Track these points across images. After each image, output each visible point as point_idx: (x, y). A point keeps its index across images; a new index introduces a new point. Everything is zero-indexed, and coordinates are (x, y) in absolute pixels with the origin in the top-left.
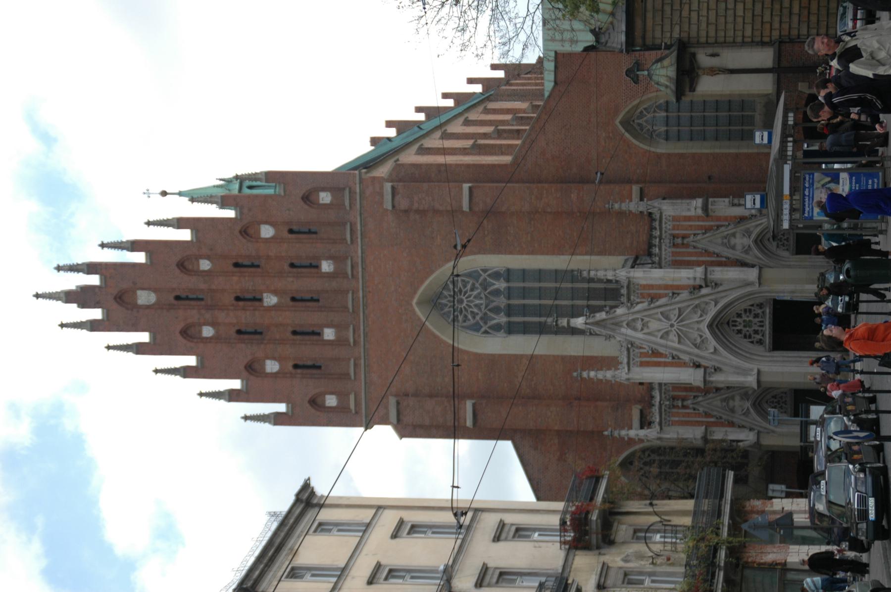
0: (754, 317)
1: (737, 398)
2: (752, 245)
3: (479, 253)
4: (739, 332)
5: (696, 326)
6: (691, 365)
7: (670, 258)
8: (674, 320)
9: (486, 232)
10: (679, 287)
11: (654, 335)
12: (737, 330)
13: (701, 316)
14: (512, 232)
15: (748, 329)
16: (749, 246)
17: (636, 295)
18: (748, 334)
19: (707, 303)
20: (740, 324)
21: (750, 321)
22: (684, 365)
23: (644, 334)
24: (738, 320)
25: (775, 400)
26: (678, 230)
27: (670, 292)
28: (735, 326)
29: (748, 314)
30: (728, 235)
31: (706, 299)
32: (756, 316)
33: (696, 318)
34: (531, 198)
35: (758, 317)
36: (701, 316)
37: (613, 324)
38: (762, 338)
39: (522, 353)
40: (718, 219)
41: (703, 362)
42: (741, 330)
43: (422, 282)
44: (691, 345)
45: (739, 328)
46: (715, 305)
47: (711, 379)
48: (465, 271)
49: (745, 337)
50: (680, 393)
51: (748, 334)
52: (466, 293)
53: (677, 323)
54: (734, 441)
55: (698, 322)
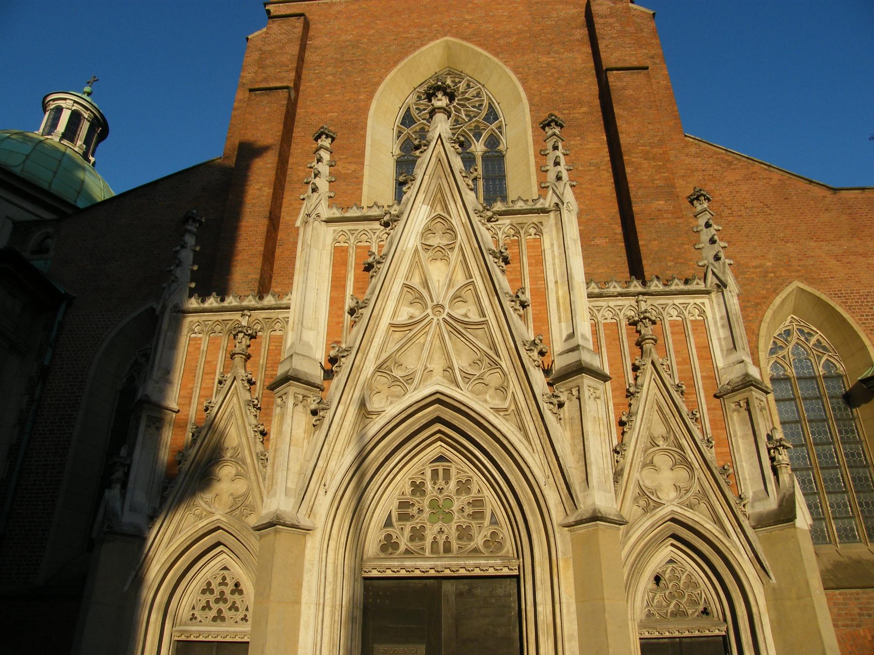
0: (459, 527)
1: (240, 486)
2: (662, 512)
3: (531, 104)
4: (418, 488)
5: (437, 365)
6: (333, 353)
7: (602, 321)
8: (452, 313)
9: (564, 112)
10: (542, 321)
11: (410, 271)
12: (422, 484)
13: (467, 377)
14: (572, 143)
15: (427, 510)
16: (660, 504)
17: (512, 232)
18: (414, 511)
19: (502, 389)
20: (441, 490)
21: (450, 514)
22: (333, 340)
23: (416, 251)
24: (453, 484)
25: (227, 590)
26: (672, 333)
27: (527, 297)
28: (435, 473)
29: (469, 510)
30: (681, 447)
31: (514, 386)
32: (464, 533)
33: (461, 362)
34: (645, 146)
35: (460, 538)
36: (467, 377)
37: (440, 189)
38: (402, 548)
39: (365, 164)
40: (721, 423)
41: (338, 380)
42: (423, 493)
43: (480, 45)
44: (384, 356)
45: (429, 485)
46: (497, 410)
47: (290, 402)
48: (496, 104)
49: (403, 505)
50: (263, 352)
51: (414, 511)
52: (463, 106)
53: (445, 320)
54: (127, 475)
55: (449, 368)
